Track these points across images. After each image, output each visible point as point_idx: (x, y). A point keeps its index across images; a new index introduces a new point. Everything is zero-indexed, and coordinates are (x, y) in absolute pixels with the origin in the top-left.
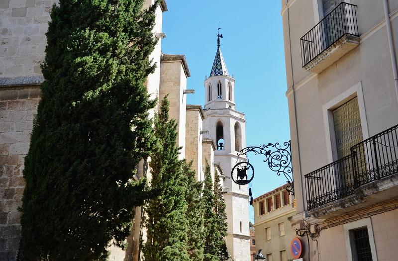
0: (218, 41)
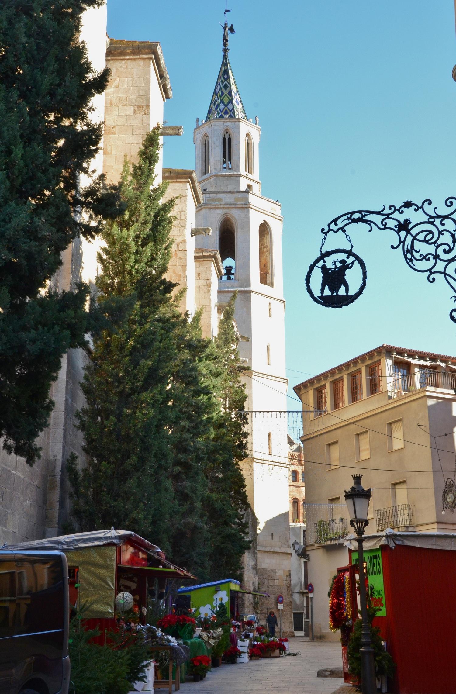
0: (225, 40)
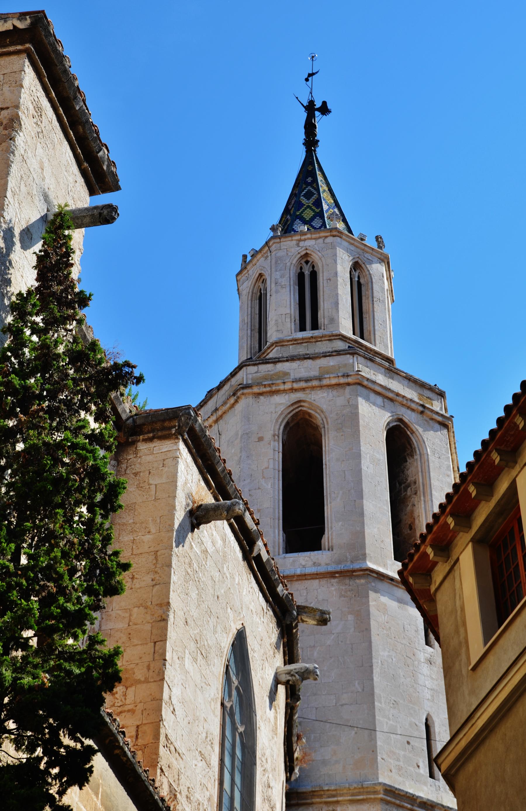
0: (310, 128)
